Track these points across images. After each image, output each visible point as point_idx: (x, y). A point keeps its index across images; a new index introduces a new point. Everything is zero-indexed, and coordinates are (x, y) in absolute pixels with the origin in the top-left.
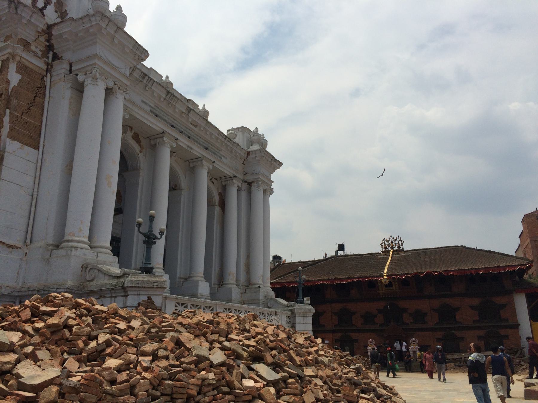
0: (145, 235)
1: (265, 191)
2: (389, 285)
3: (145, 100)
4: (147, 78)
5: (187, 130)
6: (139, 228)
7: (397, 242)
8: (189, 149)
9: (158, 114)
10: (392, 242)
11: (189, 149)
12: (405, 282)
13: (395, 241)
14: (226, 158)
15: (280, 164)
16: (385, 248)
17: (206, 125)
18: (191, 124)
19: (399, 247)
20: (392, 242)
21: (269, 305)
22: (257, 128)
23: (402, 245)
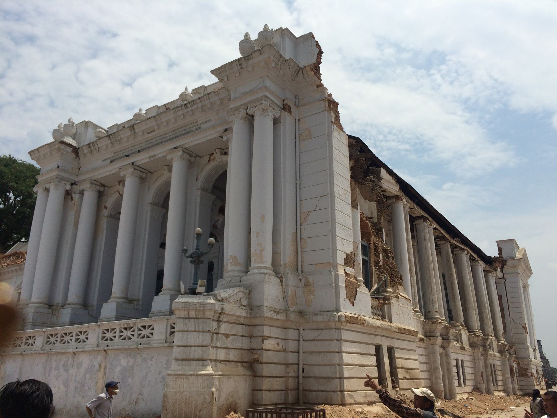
3: (104, 158)
4: (91, 145)
9: (127, 154)
14: (210, 121)
17: (156, 121)
18: (149, 133)
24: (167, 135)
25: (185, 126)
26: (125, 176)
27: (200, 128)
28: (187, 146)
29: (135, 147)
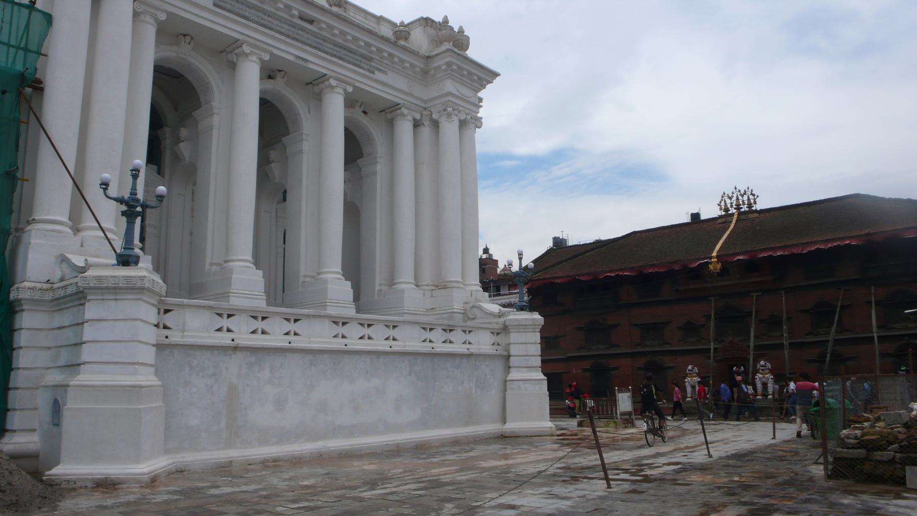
0: (120, 201)
1: (463, 124)
2: (724, 271)
5: (293, 29)
6: (105, 189)
7: (745, 198)
8: (303, 63)
10: (738, 199)
11: (303, 63)
12: (752, 265)
13: (742, 196)
15: (495, 75)
16: (726, 210)
18: (301, 18)
19: (750, 206)
20: (738, 199)
21: (471, 317)
22: (446, 17)
23: (755, 203)
24: (328, 45)
25: (355, 54)
26: (247, 55)
27: (374, 73)
28: (357, 84)
29: (266, 17)
